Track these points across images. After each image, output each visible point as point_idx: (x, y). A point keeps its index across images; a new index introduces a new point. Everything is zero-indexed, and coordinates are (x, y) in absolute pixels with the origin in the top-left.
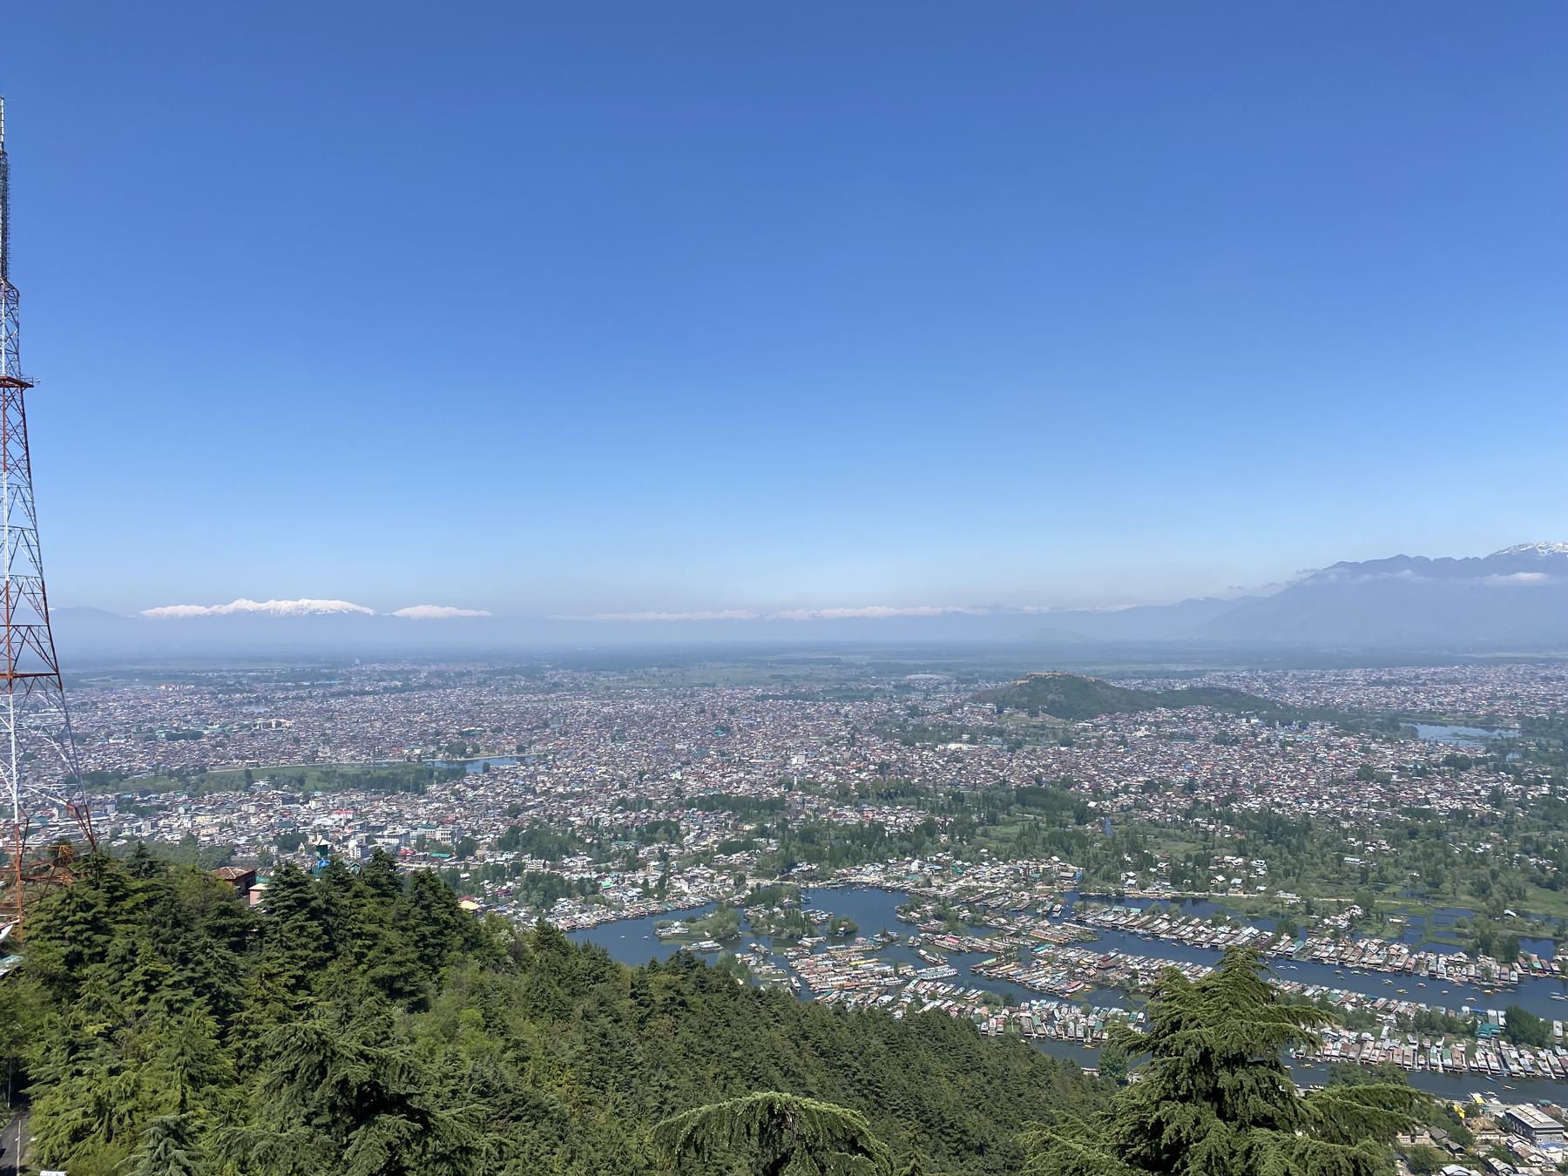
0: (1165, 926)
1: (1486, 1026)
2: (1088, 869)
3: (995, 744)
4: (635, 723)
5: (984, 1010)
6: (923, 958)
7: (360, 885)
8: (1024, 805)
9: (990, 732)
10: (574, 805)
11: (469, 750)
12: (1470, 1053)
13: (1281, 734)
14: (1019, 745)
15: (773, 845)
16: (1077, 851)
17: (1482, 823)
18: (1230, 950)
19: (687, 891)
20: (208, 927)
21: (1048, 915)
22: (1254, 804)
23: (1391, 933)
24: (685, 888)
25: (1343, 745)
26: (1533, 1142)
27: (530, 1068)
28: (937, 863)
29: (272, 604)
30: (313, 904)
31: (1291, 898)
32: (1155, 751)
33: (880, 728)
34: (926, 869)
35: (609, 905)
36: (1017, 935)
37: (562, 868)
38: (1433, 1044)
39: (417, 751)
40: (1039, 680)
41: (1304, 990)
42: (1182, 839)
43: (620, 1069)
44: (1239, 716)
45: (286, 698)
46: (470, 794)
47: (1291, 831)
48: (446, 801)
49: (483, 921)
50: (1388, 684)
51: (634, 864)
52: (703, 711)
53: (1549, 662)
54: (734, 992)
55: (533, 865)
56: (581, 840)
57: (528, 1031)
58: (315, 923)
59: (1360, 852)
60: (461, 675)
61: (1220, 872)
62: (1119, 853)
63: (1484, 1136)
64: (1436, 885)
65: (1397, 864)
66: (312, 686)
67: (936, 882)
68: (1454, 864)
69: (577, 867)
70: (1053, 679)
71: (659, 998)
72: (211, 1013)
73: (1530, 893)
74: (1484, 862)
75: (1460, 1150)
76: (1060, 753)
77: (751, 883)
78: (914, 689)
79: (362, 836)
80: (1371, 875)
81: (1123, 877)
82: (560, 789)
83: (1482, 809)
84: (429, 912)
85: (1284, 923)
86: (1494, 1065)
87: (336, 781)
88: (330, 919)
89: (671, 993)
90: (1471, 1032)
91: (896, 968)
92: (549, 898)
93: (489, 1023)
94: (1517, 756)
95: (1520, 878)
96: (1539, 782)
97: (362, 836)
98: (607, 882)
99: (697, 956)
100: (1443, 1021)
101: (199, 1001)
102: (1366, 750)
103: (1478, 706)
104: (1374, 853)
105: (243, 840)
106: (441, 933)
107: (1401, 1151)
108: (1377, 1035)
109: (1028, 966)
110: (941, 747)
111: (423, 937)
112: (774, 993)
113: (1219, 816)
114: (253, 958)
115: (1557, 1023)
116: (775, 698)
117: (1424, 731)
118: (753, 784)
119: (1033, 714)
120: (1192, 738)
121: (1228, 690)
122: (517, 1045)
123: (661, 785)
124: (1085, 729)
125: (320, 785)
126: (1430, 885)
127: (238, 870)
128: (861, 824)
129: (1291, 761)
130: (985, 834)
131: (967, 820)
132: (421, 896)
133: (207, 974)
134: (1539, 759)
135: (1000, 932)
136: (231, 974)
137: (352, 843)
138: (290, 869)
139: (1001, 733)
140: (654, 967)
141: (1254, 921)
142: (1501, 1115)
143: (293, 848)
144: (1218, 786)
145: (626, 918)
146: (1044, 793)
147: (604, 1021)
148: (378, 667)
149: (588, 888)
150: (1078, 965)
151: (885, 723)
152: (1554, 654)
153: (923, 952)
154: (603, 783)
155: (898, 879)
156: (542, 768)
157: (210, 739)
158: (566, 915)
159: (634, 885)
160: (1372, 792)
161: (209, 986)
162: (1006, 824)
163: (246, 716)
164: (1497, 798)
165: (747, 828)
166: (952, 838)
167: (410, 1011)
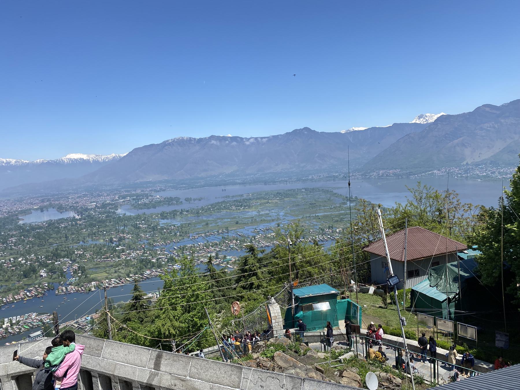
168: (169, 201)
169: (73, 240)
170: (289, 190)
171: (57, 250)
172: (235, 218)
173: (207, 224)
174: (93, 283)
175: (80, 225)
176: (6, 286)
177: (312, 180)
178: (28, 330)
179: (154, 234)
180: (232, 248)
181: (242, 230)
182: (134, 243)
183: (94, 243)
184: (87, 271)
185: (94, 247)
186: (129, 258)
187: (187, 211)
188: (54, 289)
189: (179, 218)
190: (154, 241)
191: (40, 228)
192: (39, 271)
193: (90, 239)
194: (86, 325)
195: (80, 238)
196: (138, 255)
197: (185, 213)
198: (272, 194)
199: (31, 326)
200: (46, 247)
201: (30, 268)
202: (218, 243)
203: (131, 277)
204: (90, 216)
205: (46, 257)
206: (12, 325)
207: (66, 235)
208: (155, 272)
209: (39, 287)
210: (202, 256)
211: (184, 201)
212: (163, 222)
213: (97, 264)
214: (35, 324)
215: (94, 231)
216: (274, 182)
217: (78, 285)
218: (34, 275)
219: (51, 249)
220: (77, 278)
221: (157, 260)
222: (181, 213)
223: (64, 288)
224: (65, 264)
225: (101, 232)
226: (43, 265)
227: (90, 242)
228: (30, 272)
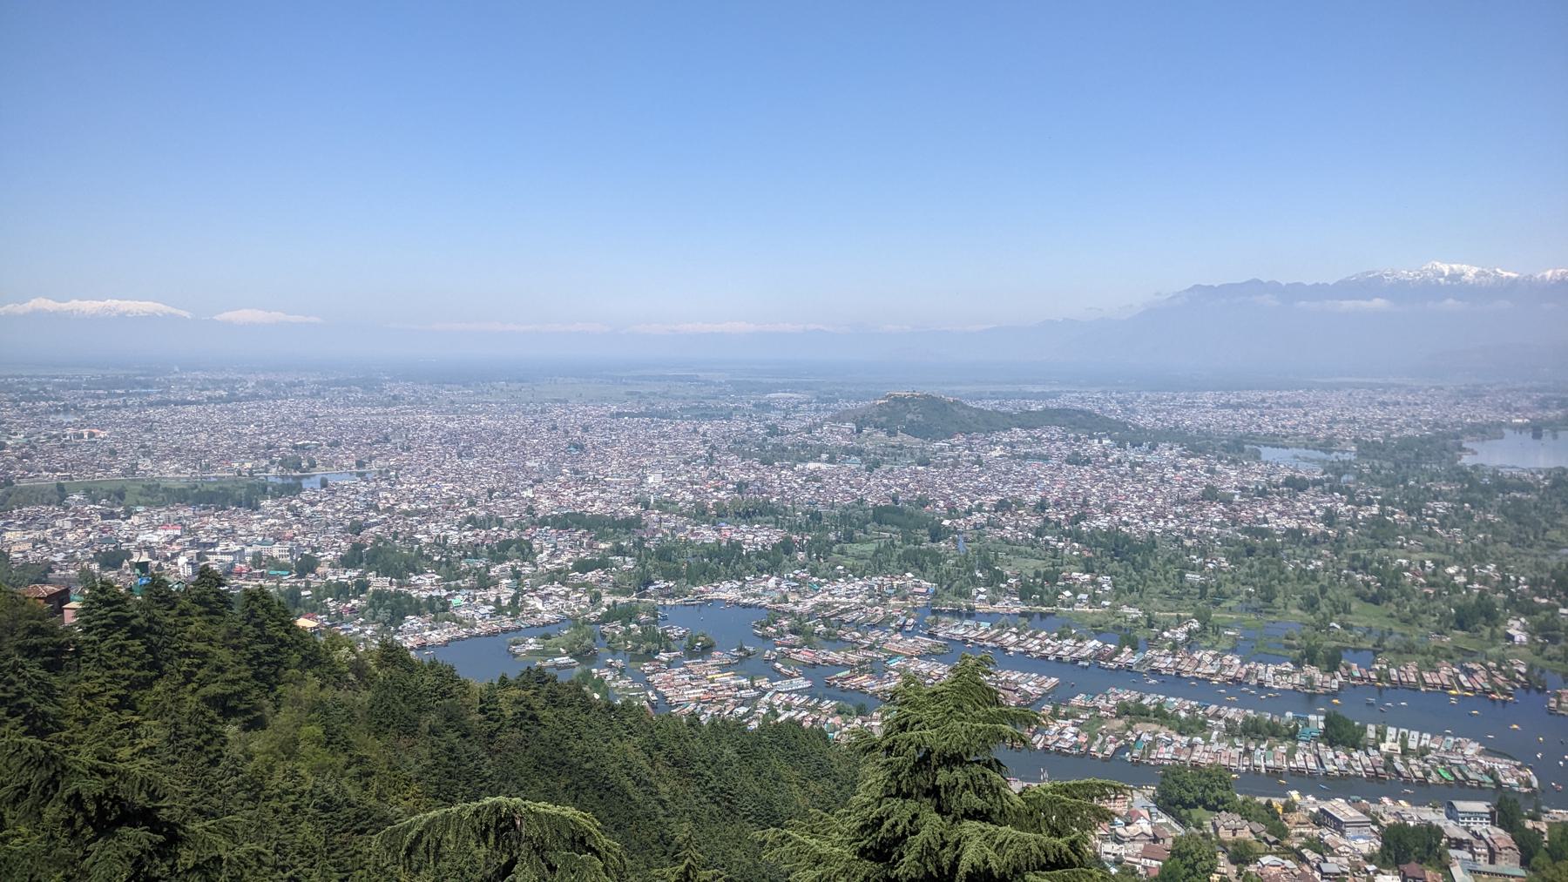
0: (1013, 639)
1: (1307, 730)
2: (940, 585)
3: (854, 463)
4: (483, 440)
5: (837, 720)
6: (778, 671)
7: (185, 603)
8: (880, 523)
9: (849, 451)
10: (420, 523)
11: (305, 464)
12: (1290, 755)
13: (1133, 454)
14: (877, 465)
15: (630, 563)
16: (931, 568)
17: (1315, 541)
18: (1075, 661)
19: (542, 608)
20: (19, 647)
21: (900, 628)
22: (1103, 522)
23: (1225, 645)
24: (539, 606)
25: (1190, 467)
26: (1343, 834)
27: (375, 785)
28: (794, 580)
29: (75, 304)
30: (134, 622)
31: (1134, 613)
32: (1009, 471)
33: (739, 447)
34: (783, 586)
35: (460, 622)
36: (871, 648)
37: (409, 586)
38: (1257, 746)
39: (248, 465)
40: (902, 400)
41: (1142, 698)
42: (1032, 556)
43: (468, 781)
44: (1092, 437)
45: (98, 407)
46: (308, 510)
47: (1137, 549)
48: (283, 517)
49: (321, 639)
50: (1236, 407)
51: (485, 582)
52: (555, 428)
53: (1386, 388)
54: (587, 705)
55: (378, 582)
56: (429, 558)
57: (372, 748)
58: (138, 642)
59: (1201, 569)
60: (292, 385)
61: (1068, 587)
62: (971, 570)
63: (1299, 829)
64: (1269, 599)
65: (1234, 580)
66: (128, 394)
67: (792, 598)
68: (1287, 579)
69: (425, 585)
70: (912, 399)
71: (509, 713)
72: (26, 734)
73: (1354, 607)
75: (1276, 843)
76: (916, 473)
77: (607, 600)
78: (774, 408)
79: (193, 552)
80: (1210, 590)
81: (974, 593)
82: (405, 506)
84: (262, 630)
85: (1127, 638)
86: (1312, 765)
87: (159, 495)
88: (154, 638)
89: (521, 708)
90: (1293, 736)
91: (752, 680)
92: (397, 616)
93: (331, 740)
94: (1351, 478)
95: (1346, 593)
96: (1370, 502)
97: (193, 552)
98: (458, 600)
99: (548, 671)
100: (1268, 726)
101: (13, 721)
102: (1211, 471)
103: (1318, 430)
104: (1214, 570)
105: (59, 557)
106: (276, 651)
107: (1223, 844)
108: (1207, 739)
109: (880, 678)
110: (799, 466)
111: (257, 655)
112: (627, 706)
113: (1068, 534)
114: (70, 678)
115: (1371, 728)
116: (631, 415)
117: (1267, 453)
118: (608, 503)
119: (892, 434)
120: (1045, 458)
121: (1082, 412)
122: (360, 760)
123: (512, 504)
124: (942, 450)
125: (142, 499)
126: (1264, 599)
127: (49, 588)
128: (719, 542)
129: (1139, 481)
130: (842, 552)
131: (822, 538)
132: (253, 614)
133: (20, 694)
134: (1372, 481)
135: (854, 645)
136: (47, 694)
137: (182, 560)
138: (107, 586)
139: (859, 453)
140: (504, 683)
141: (1098, 634)
142: (1315, 810)
143: (116, 565)
144: (1069, 505)
145: (478, 636)
146: (901, 511)
147: (452, 736)
148: (200, 375)
149: (438, 606)
150: (929, 676)
151: (744, 442)
152: (1392, 380)
153: (778, 665)
154: (451, 501)
155: (755, 596)
156: (384, 484)
157: (14, 449)
158: (414, 634)
159: (486, 602)
160: (1215, 512)
161: (24, 706)
162: (862, 542)
163: (53, 426)
164: (1330, 518)
165: (603, 546)
166: (809, 555)
167: (246, 729)
191: (1525, 487)
199: (1460, 776)
200: (1535, 551)
201: (1478, 604)
205: (1534, 584)
206: (1406, 752)
209: (1499, 669)
214: (1471, 776)
218: (1488, 630)
226: (1521, 606)
228: (1475, 616)
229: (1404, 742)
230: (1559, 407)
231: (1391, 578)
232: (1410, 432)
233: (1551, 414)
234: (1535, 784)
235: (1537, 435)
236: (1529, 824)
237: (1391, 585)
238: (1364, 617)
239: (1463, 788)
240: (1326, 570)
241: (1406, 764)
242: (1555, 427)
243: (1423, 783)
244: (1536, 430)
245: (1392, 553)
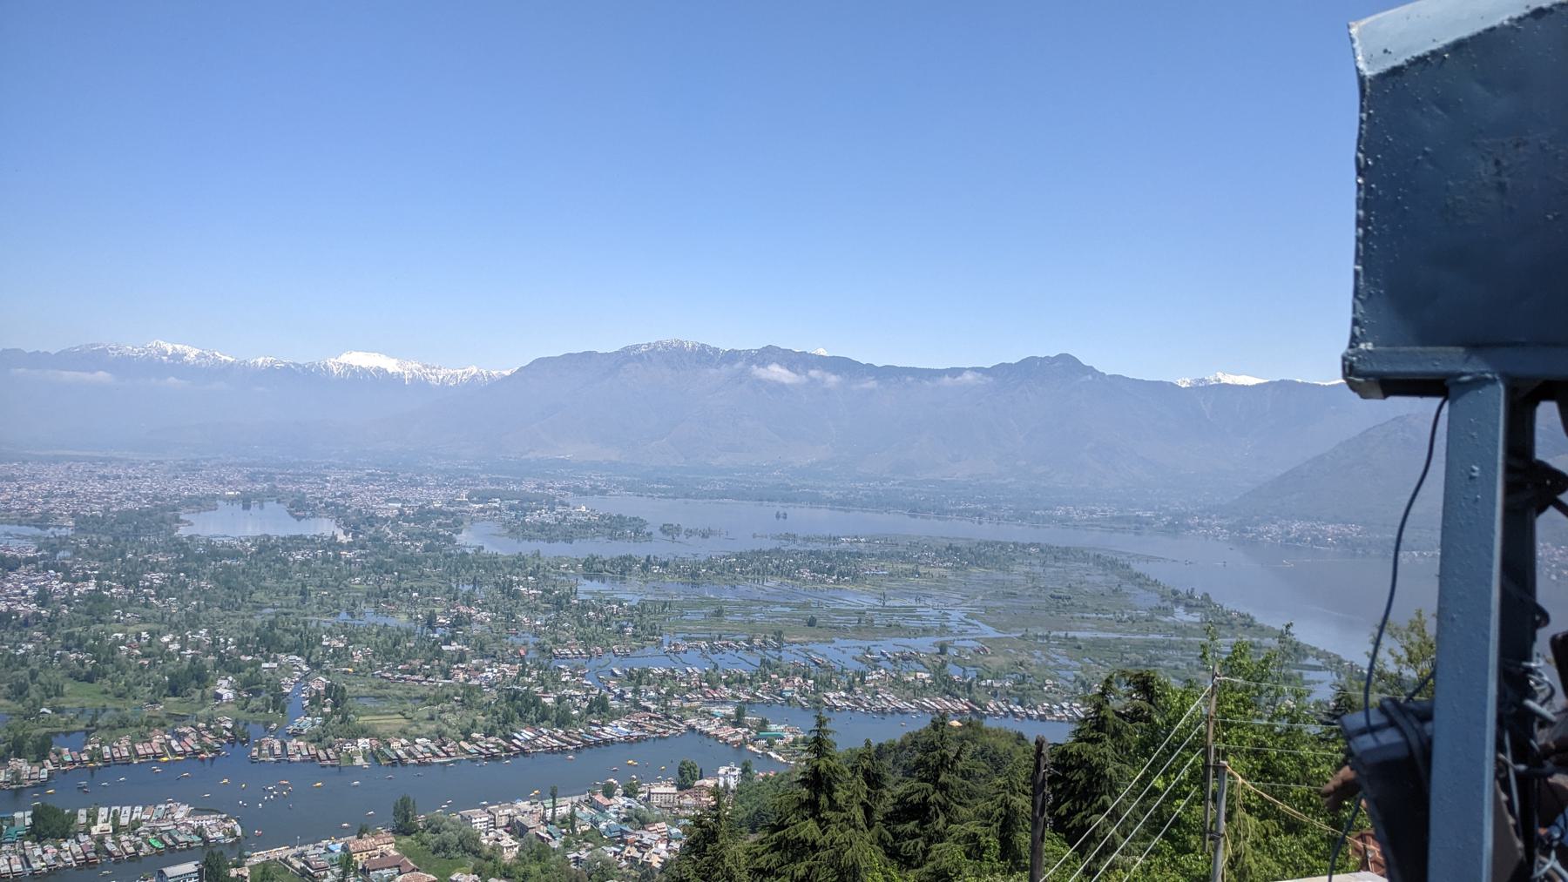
17: (26, 623)
53: (107, 461)
73: (67, 688)
74: (24, 664)
83: (27, 609)
94: (68, 554)
96: (86, 578)
134: (92, 557)
164: (43, 598)
168: (615, 526)
169: (321, 603)
170: (987, 544)
171: (272, 625)
172: (806, 606)
173: (719, 613)
174: (363, 743)
175: (348, 562)
176: (117, 710)
177: (1063, 522)
178: (159, 853)
179: (559, 619)
180: (788, 700)
181: (823, 648)
182: (495, 640)
183: (382, 621)
184: (349, 703)
185: (378, 634)
186: (476, 682)
187: (665, 565)
188: (248, 741)
189: (634, 581)
190: (556, 641)
191: (235, 555)
192: (214, 682)
193: (369, 610)
194: (325, 868)
195: (343, 602)
196: (504, 676)
197: (656, 569)
198: (930, 549)
199: (170, 842)
200: (242, 613)
201: (190, 669)
202: (746, 675)
203: (474, 741)
204: (379, 539)
205: (241, 644)
206: (117, 829)
207: (304, 586)
208: (549, 737)
209: (208, 728)
210: (694, 710)
211: (657, 534)
212: (587, 588)
213: (380, 686)
214: (181, 839)
215: (384, 587)
216: (941, 513)
217: (317, 739)
218: (199, 692)
219: (257, 621)
220: (319, 720)
221: (559, 700)
222: (645, 568)
223: (277, 744)
224: (290, 672)
225: (405, 590)
226: (228, 665)
227: (369, 616)
228: (187, 681)
229: (116, 818)
230: (266, 480)
231: (106, 655)
232: (130, 505)
233: (259, 487)
234: (239, 833)
235: (246, 507)
236: (234, 873)
237: (105, 661)
238: (77, 697)
239: (174, 853)
240: (37, 653)
241: (117, 842)
242: (261, 498)
243: (134, 857)
244: (246, 502)
245: (108, 628)
